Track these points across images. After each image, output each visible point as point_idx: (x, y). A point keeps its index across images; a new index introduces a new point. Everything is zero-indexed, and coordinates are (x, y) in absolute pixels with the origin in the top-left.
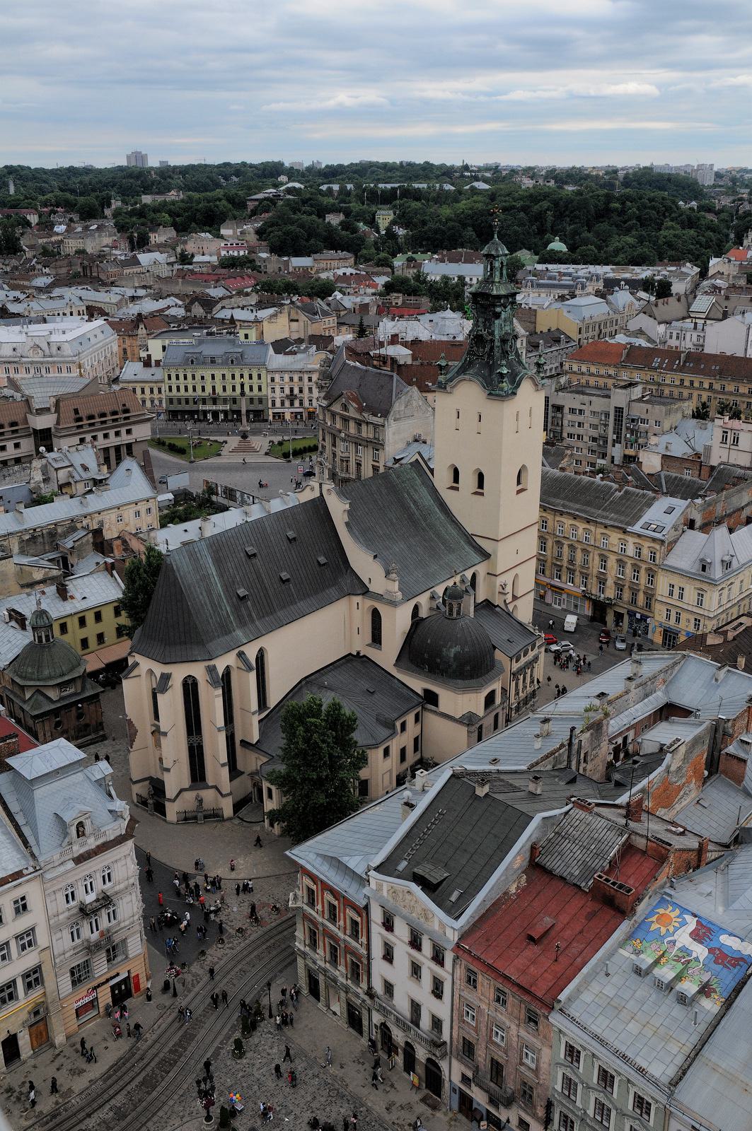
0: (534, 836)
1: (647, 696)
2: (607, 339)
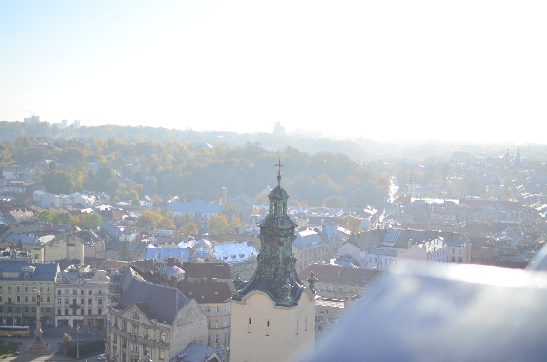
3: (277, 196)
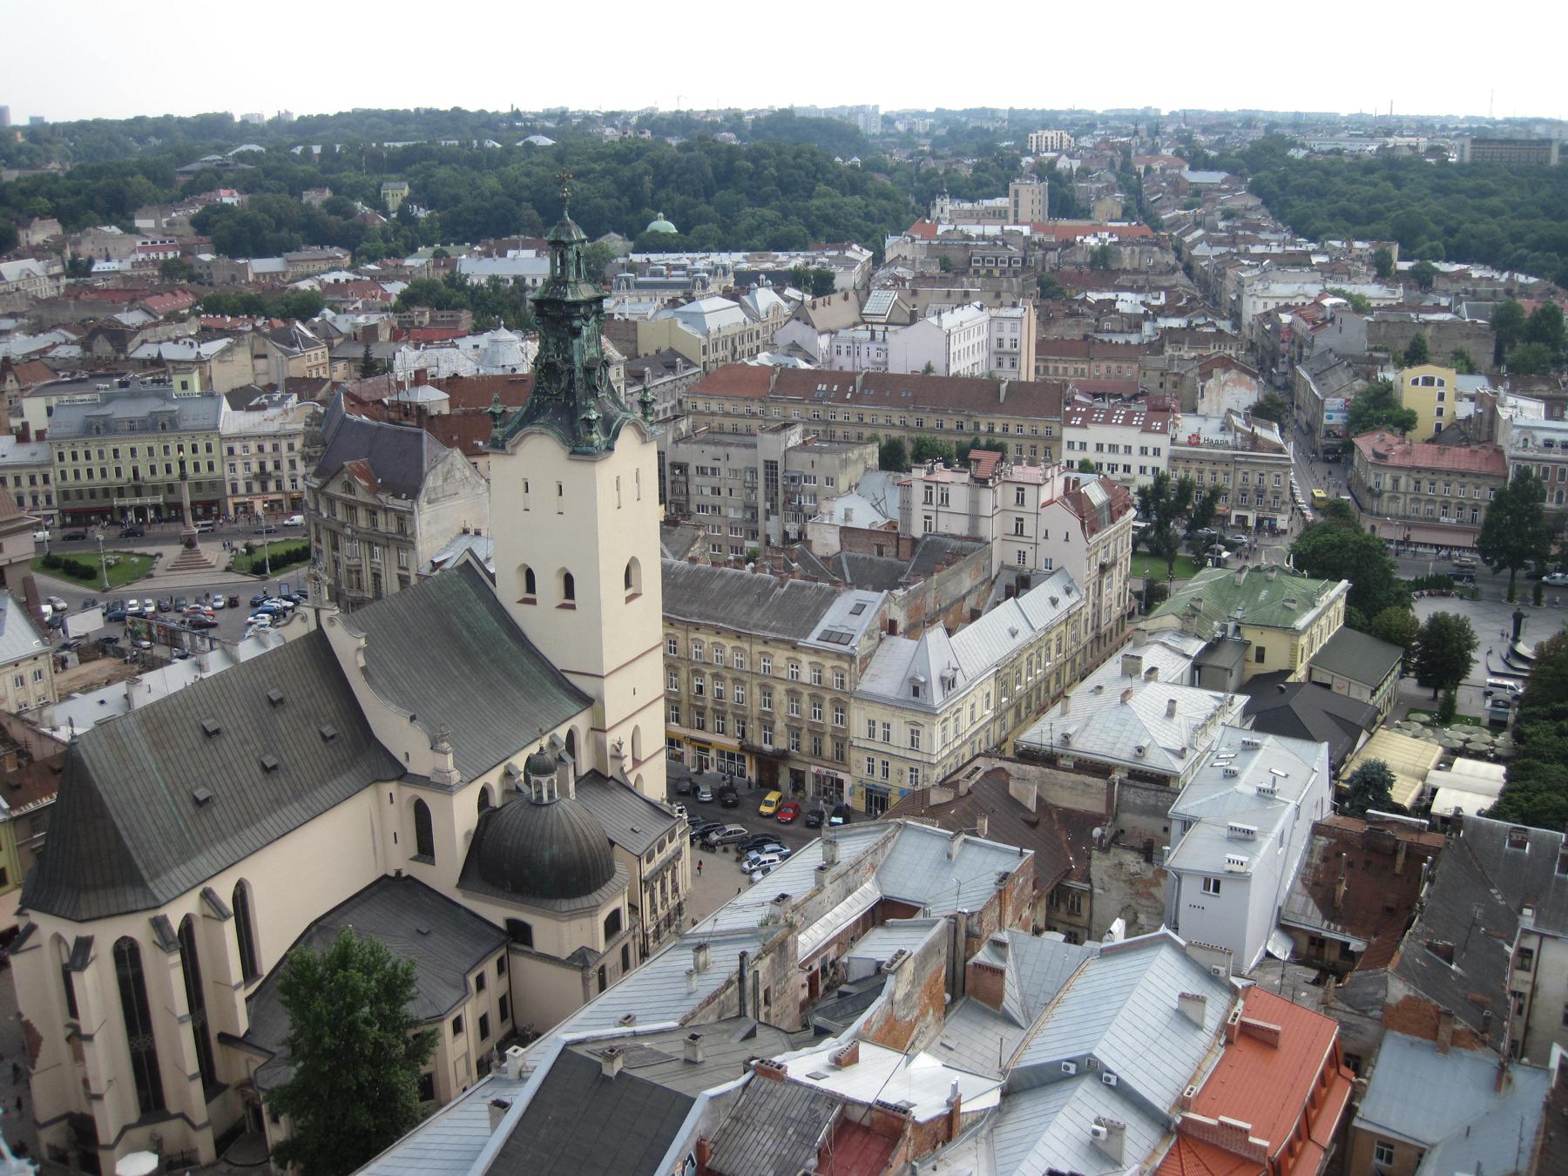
0: (702, 1127)
1: (849, 892)
2: (745, 360)
3: (563, 238)
